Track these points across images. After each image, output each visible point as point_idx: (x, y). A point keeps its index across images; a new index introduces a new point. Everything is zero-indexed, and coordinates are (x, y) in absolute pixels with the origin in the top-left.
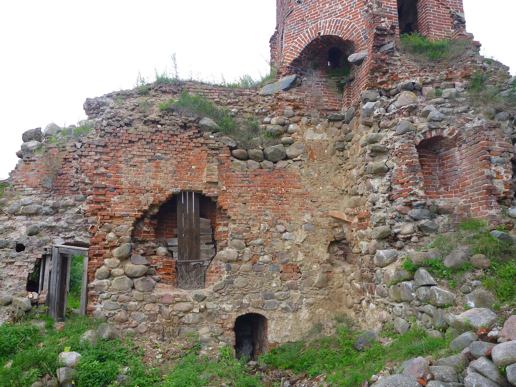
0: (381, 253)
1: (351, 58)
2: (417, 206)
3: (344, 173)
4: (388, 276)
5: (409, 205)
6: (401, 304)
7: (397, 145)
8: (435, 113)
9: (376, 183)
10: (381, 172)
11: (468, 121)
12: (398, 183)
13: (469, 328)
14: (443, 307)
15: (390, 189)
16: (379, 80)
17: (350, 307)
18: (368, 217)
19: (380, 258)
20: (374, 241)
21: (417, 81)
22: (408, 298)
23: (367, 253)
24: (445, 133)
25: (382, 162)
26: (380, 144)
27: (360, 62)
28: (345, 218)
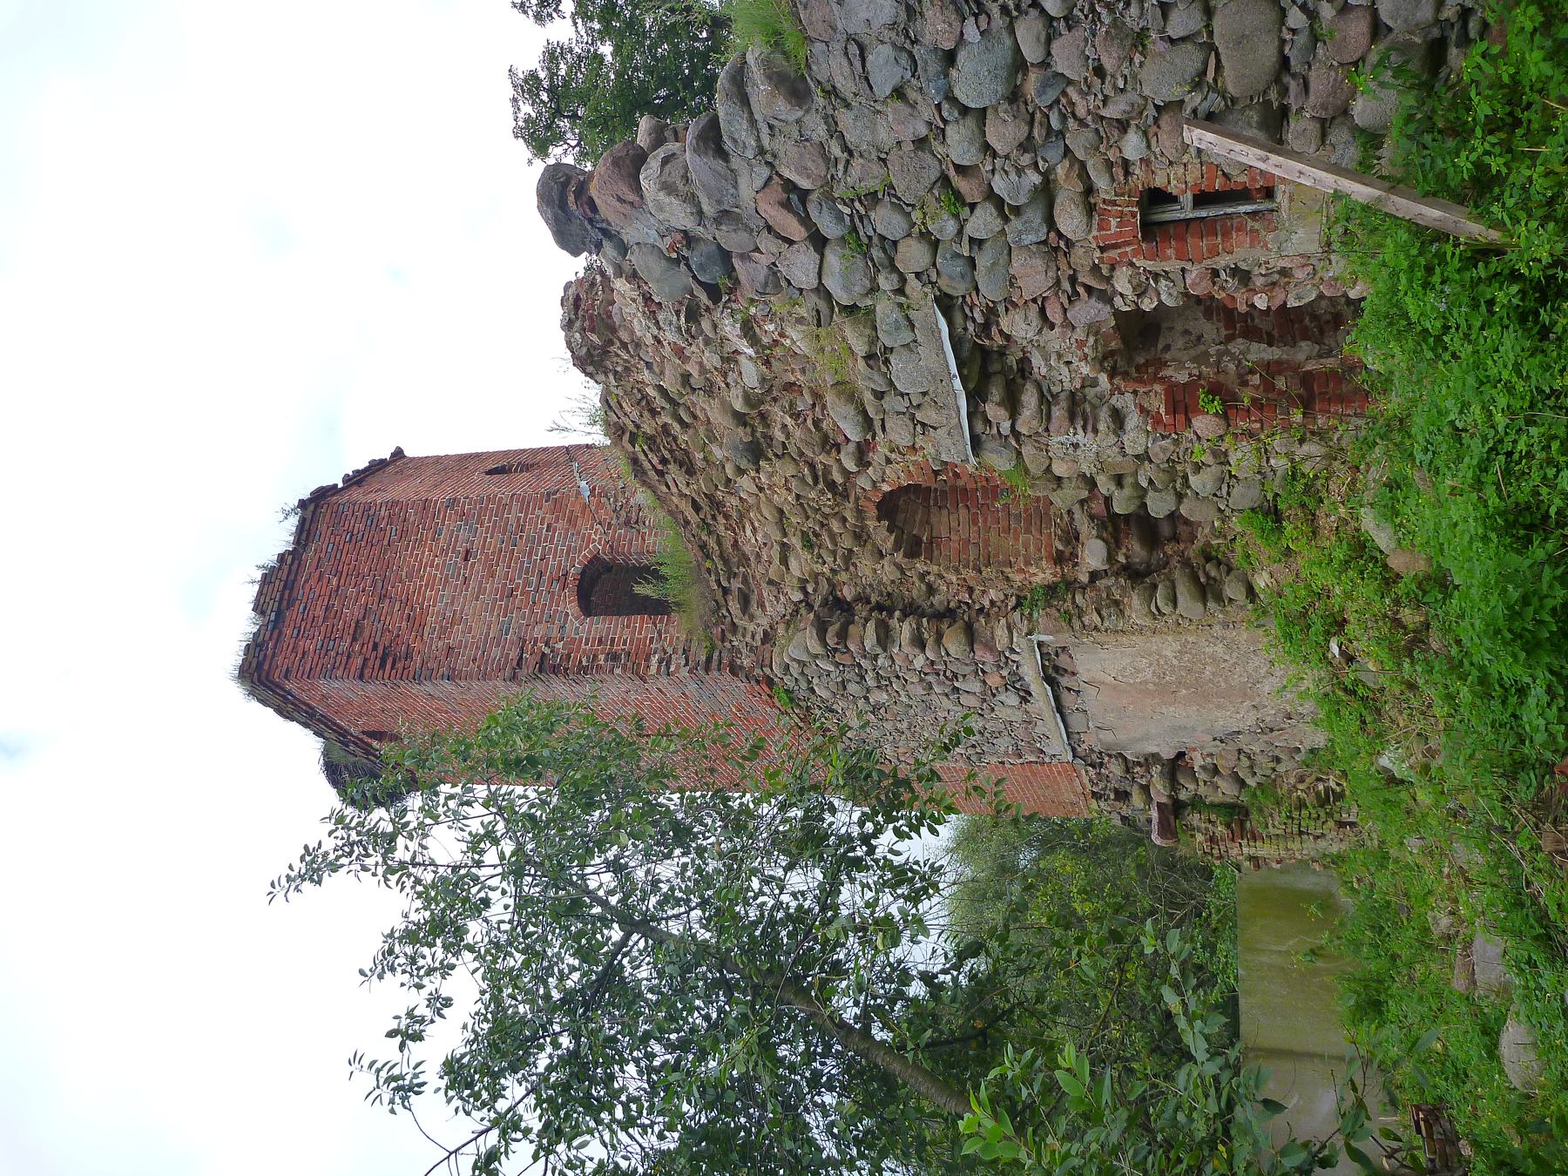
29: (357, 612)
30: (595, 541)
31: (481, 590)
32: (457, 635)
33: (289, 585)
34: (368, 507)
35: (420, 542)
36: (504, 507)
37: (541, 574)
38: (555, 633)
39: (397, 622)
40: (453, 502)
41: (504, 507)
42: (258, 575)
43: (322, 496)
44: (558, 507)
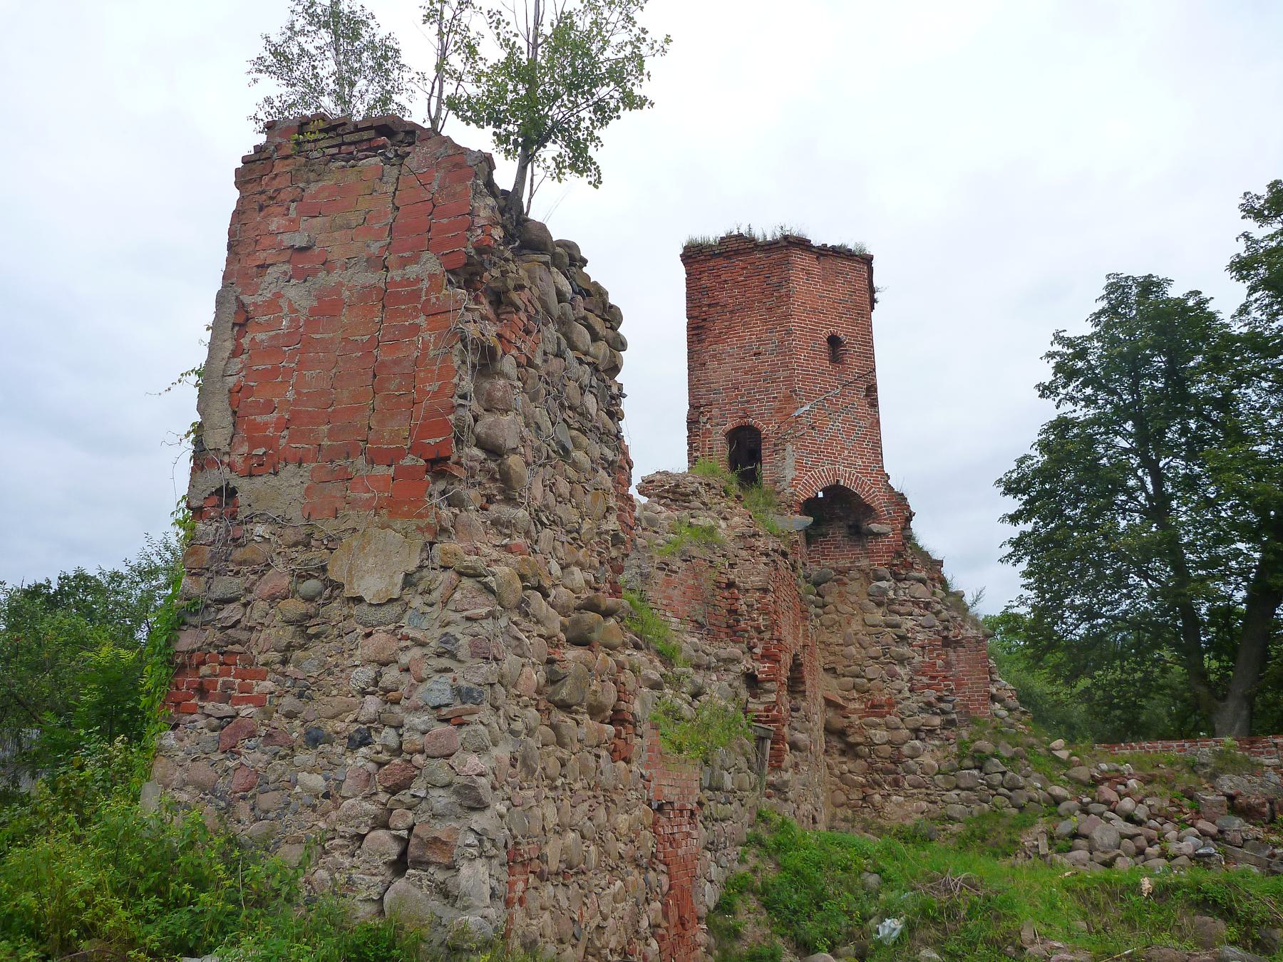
0: (918, 743)
1: (875, 527)
2: (949, 702)
3: (822, 646)
4: (932, 767)
5: (940, 699)
6: (957, 792)
7: (920, 637)
8: (945, 614)
9: (897, 668)
10: (902, 660)
11: (962, 627)
12: (924, 674)
13: (1065, 799)
14: (1022, 788)
15: (911, 679)
16: (895, 562)
17: (842, 805)
18: (892, 706)
19: (913, 748)
20: (905, 733)
21: (923, 575)
22: (972, 784)
23: (889, 742)
24: (951, 634)
25: (905, 650)
26: (902, 632)
27: (878, 535)
28: (841, 701)
29: (723, 302)
30: (767, 429)
31: (736, 370)
32: (712, 365)
33: (737, 253)
34: (788, 280)
35: (765, 321)
36: (785, 366)
37: (748, 402)
38: (715, 421)
39: (717, 327)
40: (789, 332)
41: (785, 366)
42: (743, 230)
43: (801, 244)
44: (788, 399)
